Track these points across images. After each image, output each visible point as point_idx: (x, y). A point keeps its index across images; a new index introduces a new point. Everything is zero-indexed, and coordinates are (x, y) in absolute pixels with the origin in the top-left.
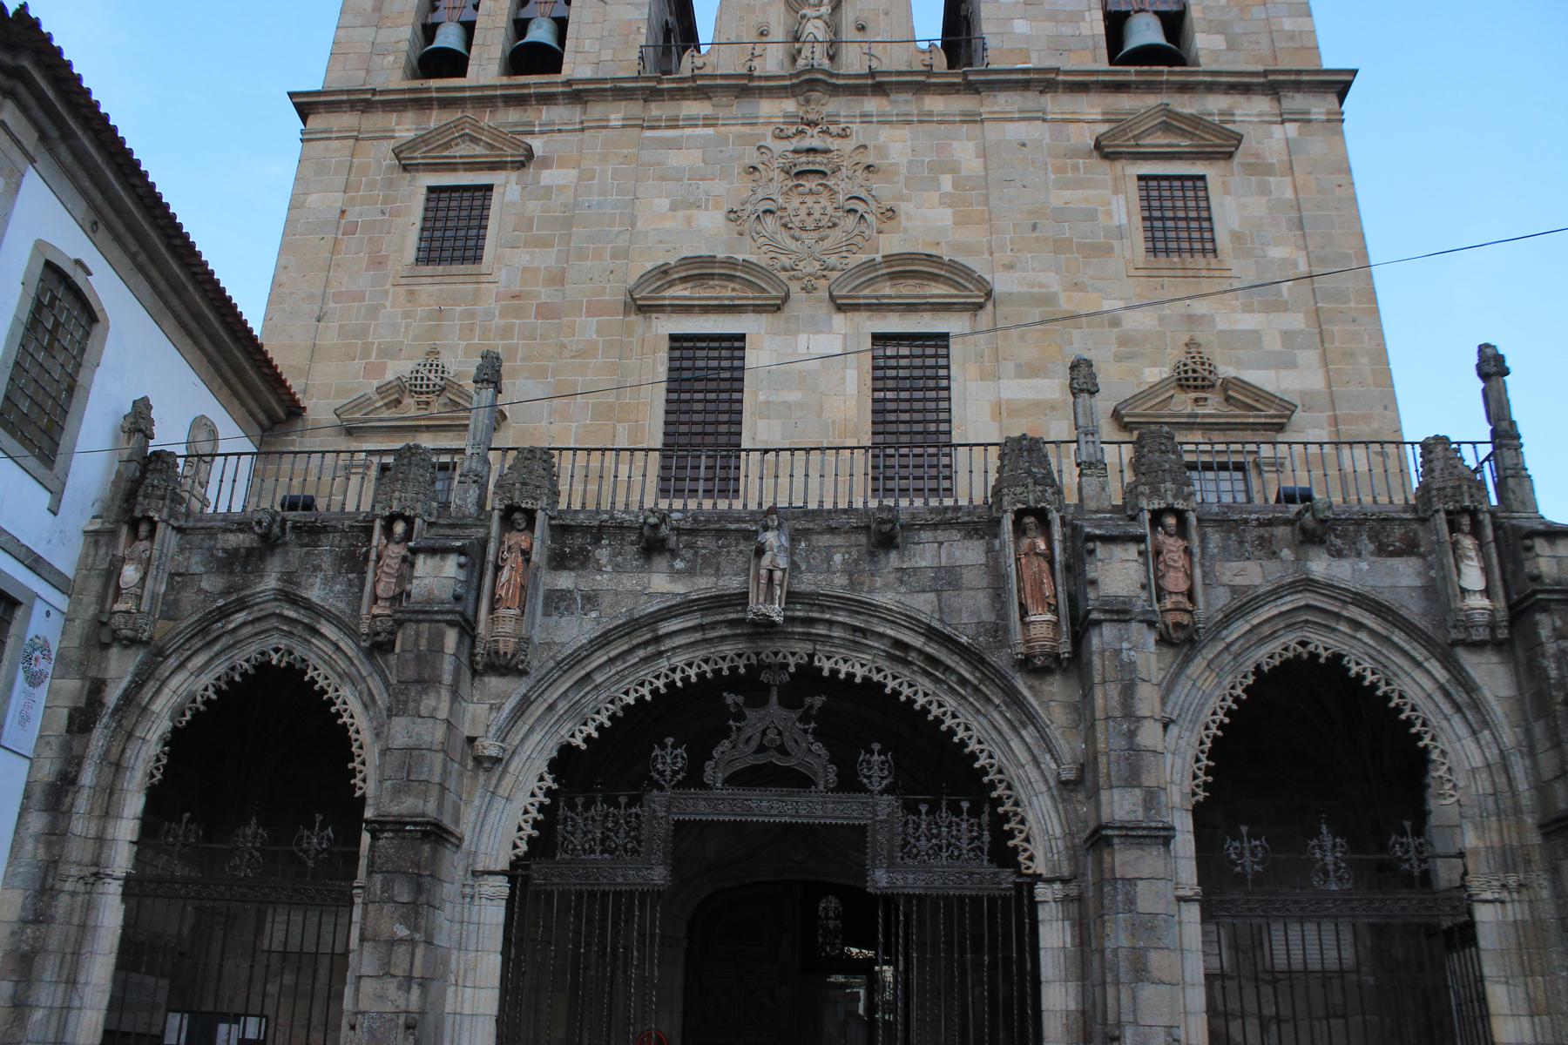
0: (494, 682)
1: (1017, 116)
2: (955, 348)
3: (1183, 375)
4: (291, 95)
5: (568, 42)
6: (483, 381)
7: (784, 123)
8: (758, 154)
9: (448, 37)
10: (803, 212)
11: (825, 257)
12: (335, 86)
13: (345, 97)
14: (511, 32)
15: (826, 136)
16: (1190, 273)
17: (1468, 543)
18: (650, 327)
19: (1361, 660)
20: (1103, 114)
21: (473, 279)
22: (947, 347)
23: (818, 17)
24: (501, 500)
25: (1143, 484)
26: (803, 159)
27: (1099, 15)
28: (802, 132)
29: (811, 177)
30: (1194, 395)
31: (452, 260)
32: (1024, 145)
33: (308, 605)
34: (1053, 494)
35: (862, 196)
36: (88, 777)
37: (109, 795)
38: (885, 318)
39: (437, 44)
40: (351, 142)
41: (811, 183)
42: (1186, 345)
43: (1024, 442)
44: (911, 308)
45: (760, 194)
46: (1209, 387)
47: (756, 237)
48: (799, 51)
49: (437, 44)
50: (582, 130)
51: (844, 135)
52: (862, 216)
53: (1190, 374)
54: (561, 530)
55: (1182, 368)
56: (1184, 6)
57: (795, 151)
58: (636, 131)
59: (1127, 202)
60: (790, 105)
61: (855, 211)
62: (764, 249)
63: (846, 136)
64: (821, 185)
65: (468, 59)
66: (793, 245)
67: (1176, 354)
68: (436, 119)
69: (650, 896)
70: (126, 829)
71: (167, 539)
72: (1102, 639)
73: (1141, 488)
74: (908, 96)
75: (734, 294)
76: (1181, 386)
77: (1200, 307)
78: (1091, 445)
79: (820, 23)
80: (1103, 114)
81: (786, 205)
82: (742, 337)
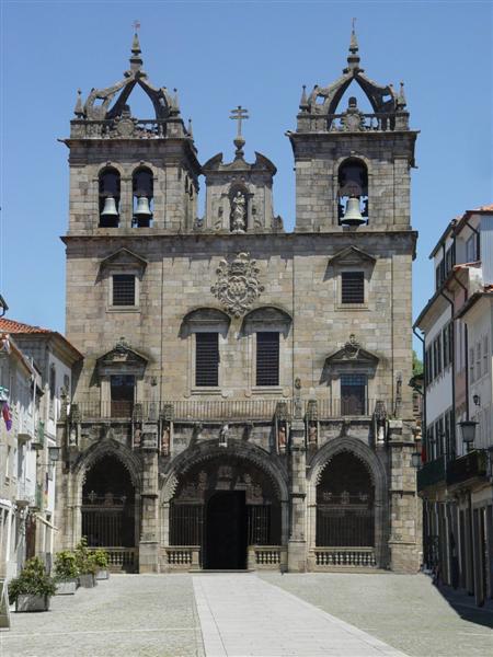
0: (163, 460)
17: (382, 428)
19: (359, 453)
33: (117, 443)
36: (70, 484)
37: (74, 487)
39: (105, 212)
41: (237, 278)
49: (105, 212)
54: (176, 426)
67: (348, 340)
69: (200, 506)
70: (79, 495)
71: (79, 427)
72: (294, 453)
77: (356, 321)
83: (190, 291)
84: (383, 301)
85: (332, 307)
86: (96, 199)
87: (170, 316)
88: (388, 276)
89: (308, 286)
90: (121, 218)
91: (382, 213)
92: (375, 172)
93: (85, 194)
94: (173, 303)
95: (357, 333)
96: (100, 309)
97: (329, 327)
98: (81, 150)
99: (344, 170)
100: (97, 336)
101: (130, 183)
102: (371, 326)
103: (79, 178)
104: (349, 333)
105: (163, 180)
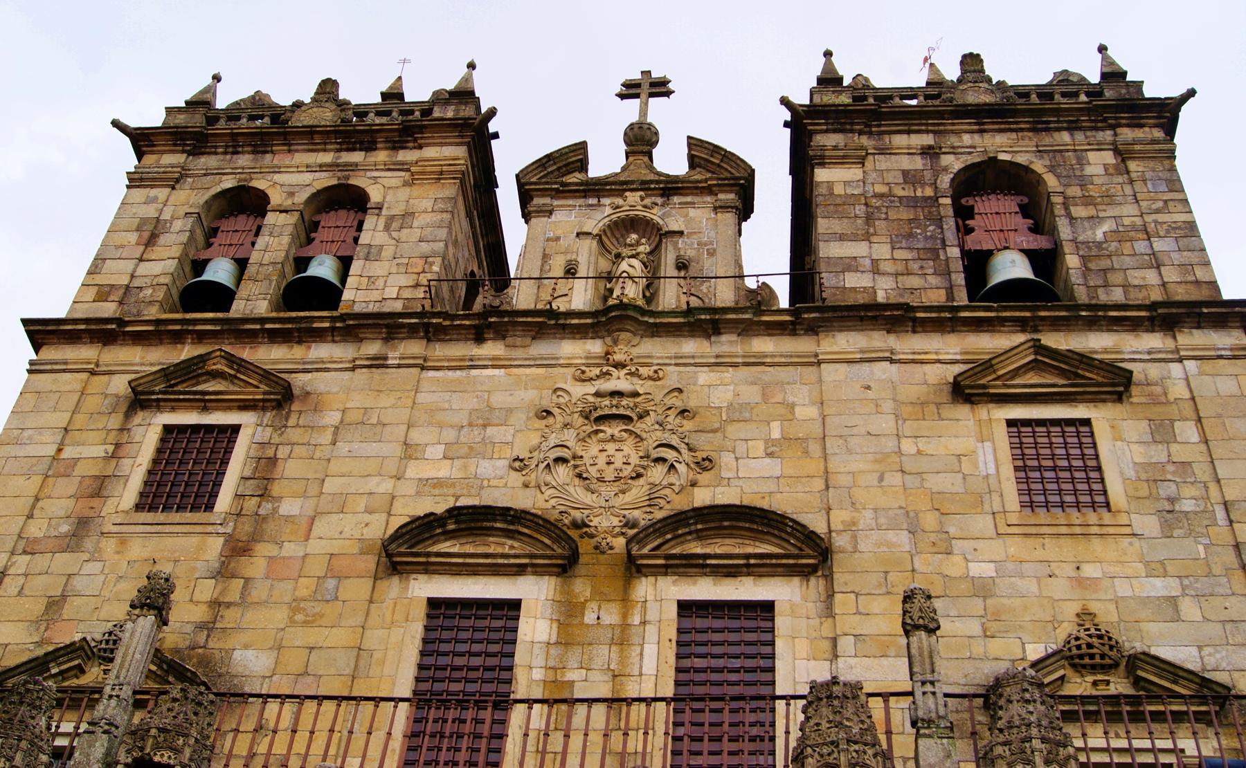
1: (859, 356)
2: (782, 623)
3: (1075, 651)
4: (26, 322)
5: (351, 281)
6: (142, 607)
7: (588, 365)
8: (554, 397)
9: (220, 271)
10: (602, 460)
11: (626, 512)
12: (79, 315)
13: (83, 327)
14: (289, 269)
15: (635, 380)
16: (1078, 530)
18: (407, 589)
20: (961, 353)
21: (199, 529)
22: (772, 619)
23: (633, 256)
24: (128, 752)
25: (1004, 744)
26: (607, 402)
27: (954, 252)
28: (608, 373)
29: (614, 423)
30: (1090, 679)
31: (181, 508)
32: (868, 388)
34: (875, 755)
35: (674, 443)
38: (695, 584)
40: (84, 376)
42: (1078, 615)
43: (835, 688)
44: (730, 572)
45: (553, 440)
46: (1110, 667)
47: (543, 490)
48: (611, 291)
50: (353, 369)
51: (655, 378)
52: (672, 466)
53: (1084, 650)
55: (1073, 643)
56: (1056, 244)
57: (598, 394)
58: (416, 371)
59: (995, 450)
60: (595, 347)
61: (664, 460)
62: (553, 502)
63: (659, 379)
64: (625, 431)
65: (235, 293)
66: (588, 498)
68: (187, 352)
73: (999, 750)
74: (733, 337)
75: (513, 552)
76: (1074, 666)
77: (1090, 571)
78: (930, 695)
79: (635, 262)
80: (961, 353)
81: (580, 453)
82: (515, 605)
83: (428, 472)
84: (1187, 505)
85: (983, 524)
86: (176, 251)
87: (335, 547)
88: (1188, 431)
89: (882, 458)
90: (243, 292)
91: (1116, 278)
92: (1074, 191)
93: (151, 241)
94: (362, 503)
95: (1107, 616)
96: (83, 525)
97: (982, 589)
98: (172, 159)
99: (963, 201)
100: (38, 607)
101: (292, 219)
102: (1159, 587)
103: (151, 211)
104: (1071, 609)
105: (397, 211)
